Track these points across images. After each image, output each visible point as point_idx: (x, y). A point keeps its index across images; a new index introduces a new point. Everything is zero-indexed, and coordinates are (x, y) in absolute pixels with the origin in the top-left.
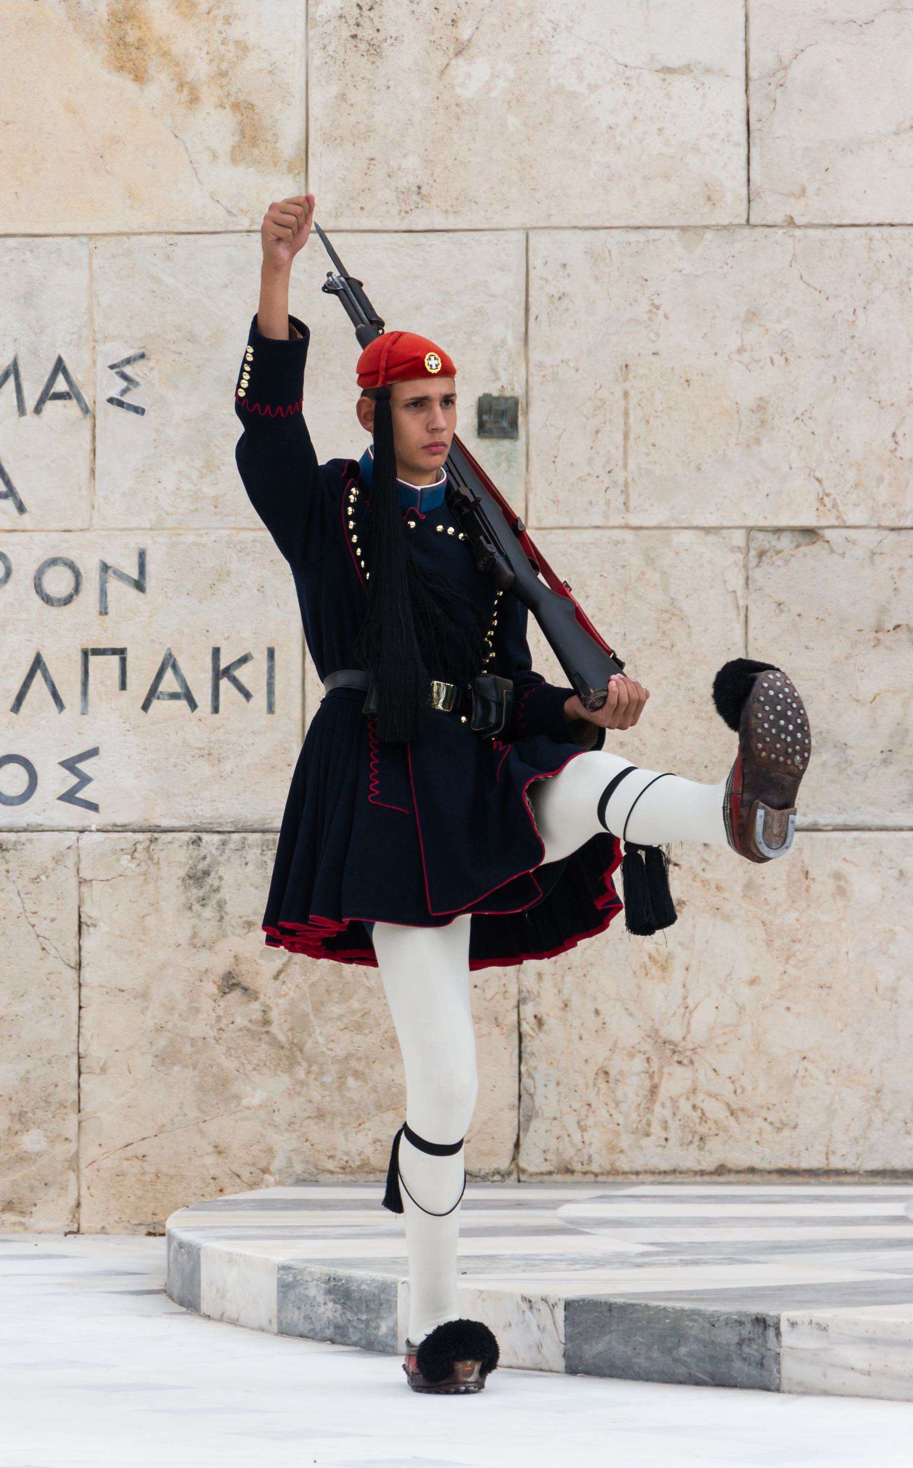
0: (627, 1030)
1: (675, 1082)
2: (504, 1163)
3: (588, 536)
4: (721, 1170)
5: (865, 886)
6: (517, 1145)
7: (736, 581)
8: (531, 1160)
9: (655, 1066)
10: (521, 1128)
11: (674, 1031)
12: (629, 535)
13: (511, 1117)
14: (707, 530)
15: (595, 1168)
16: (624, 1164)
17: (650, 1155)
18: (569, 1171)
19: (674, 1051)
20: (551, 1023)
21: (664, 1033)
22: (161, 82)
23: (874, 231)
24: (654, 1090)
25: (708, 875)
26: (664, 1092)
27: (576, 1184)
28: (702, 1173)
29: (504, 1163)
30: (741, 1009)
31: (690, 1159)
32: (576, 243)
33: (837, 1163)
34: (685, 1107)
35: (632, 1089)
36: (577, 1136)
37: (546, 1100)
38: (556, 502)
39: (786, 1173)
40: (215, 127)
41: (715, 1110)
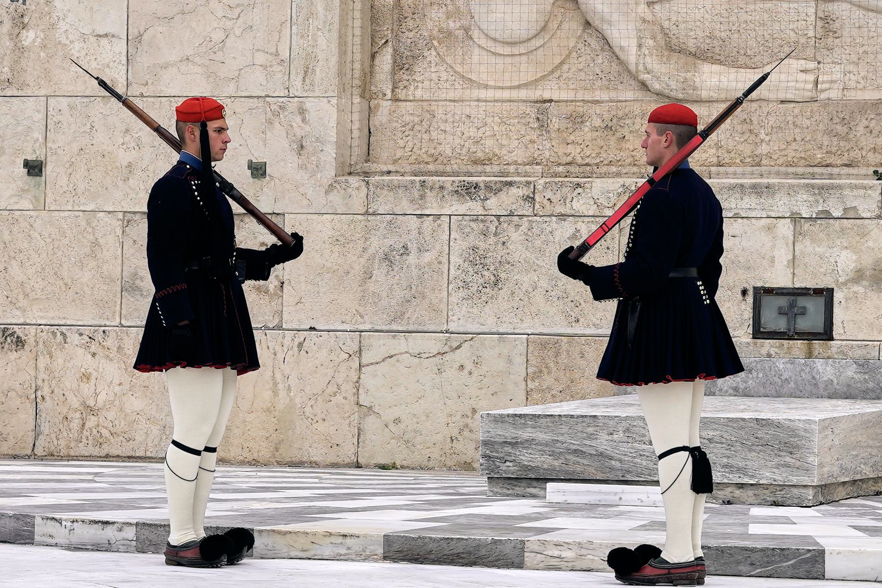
0: (75, 402)
1: (91, 422)
2: (29, 452)
3: (66, 214)
4: (107, 457)
6: (34, 445)
7: (119, 232)
8: (39, 451)
9: (84, 415)
10: (36, 439)
11: (91, 403)
12: (81, 214)
13: (31, 435)
14: (110, 212)
15: (62, 454)
16: (72, 453)
17: (83, 450)
18: (52, 455)
19: (92, 411)
20: (47, 398)
21: (88, 403)
23: (171, 99)
24: (83, 425)
25: (105, 343)
26: (89, 424)
27: (55, 460)
28: (100, 457)
29: (29, 452)
30: (116, 394)
31: (96, 452)
32: (64, 101)
33: (149, 454)
34: (95, 432)
35: (75, 424)
36: (55, 443)
38: (55, 201)
39: (130, 458)
41: (105, 433)
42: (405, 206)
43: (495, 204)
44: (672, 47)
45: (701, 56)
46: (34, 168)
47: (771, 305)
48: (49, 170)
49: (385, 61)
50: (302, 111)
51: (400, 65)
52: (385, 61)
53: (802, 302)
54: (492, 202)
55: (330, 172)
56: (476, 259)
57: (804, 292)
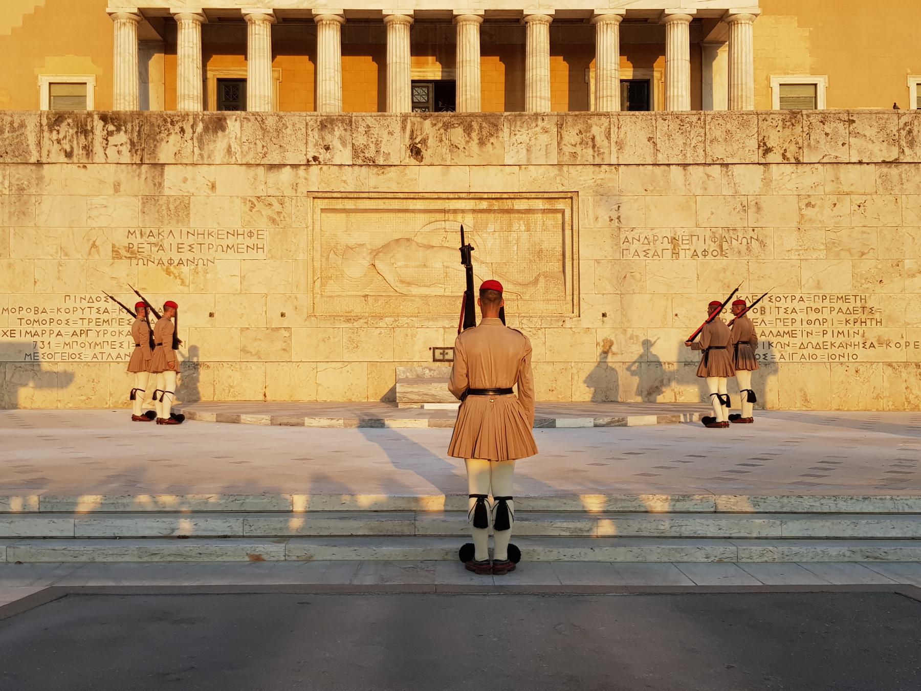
5: (254, 368)
19: (232, 387)
22: (172, 276)
35: (227, 391)
37: (217, 392)
40: (178, 281)
42: (329, 325)
43: (356, 324)
44: (402, 282)
45: (409, 284)
46: (211, 315)
47: (438, 352)
48: (216, 315)
49: (318, 283)
50: (296, 298)
51: (322, 284)
52: (318, 283)
53: (446, 351)
54: (355, 324)
55: (305, 316)
56: (351, 340)
57: (447, 348)
